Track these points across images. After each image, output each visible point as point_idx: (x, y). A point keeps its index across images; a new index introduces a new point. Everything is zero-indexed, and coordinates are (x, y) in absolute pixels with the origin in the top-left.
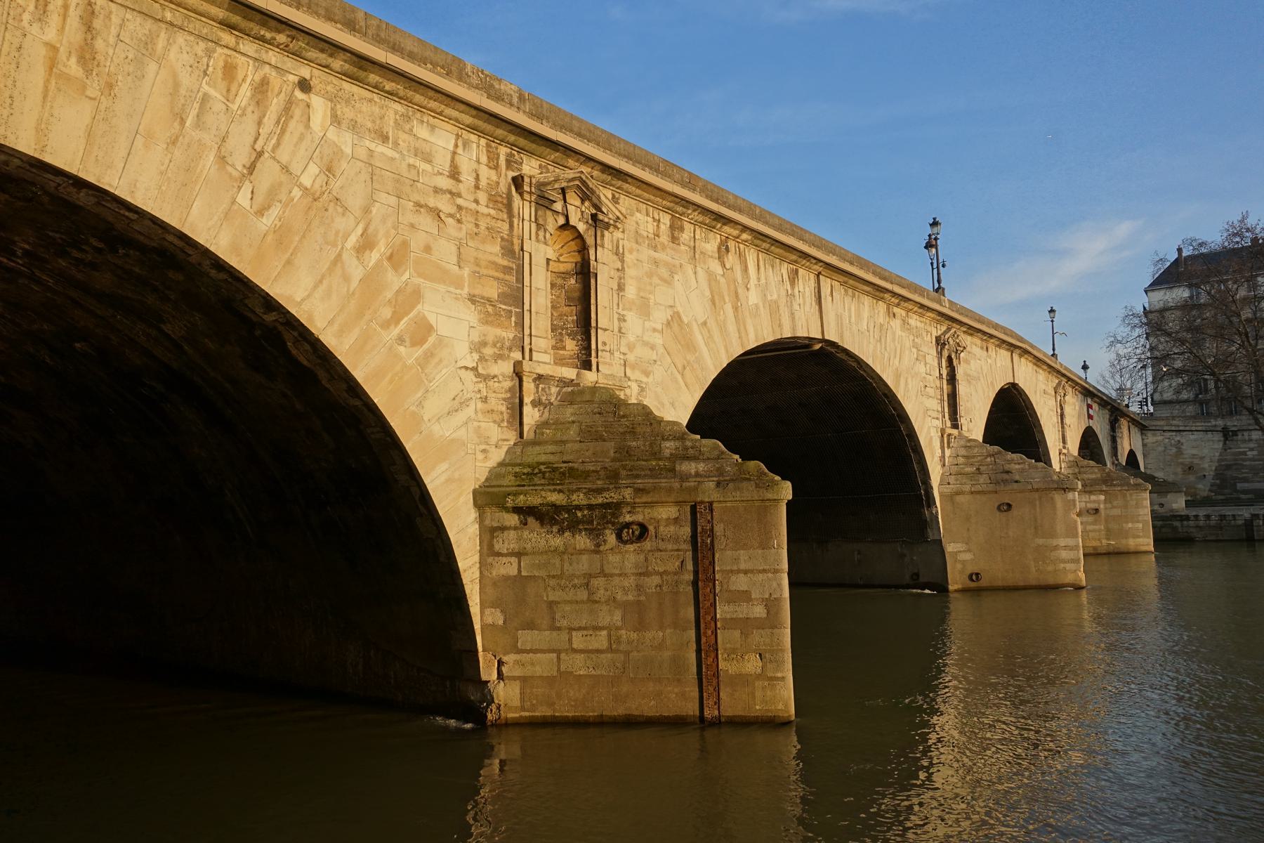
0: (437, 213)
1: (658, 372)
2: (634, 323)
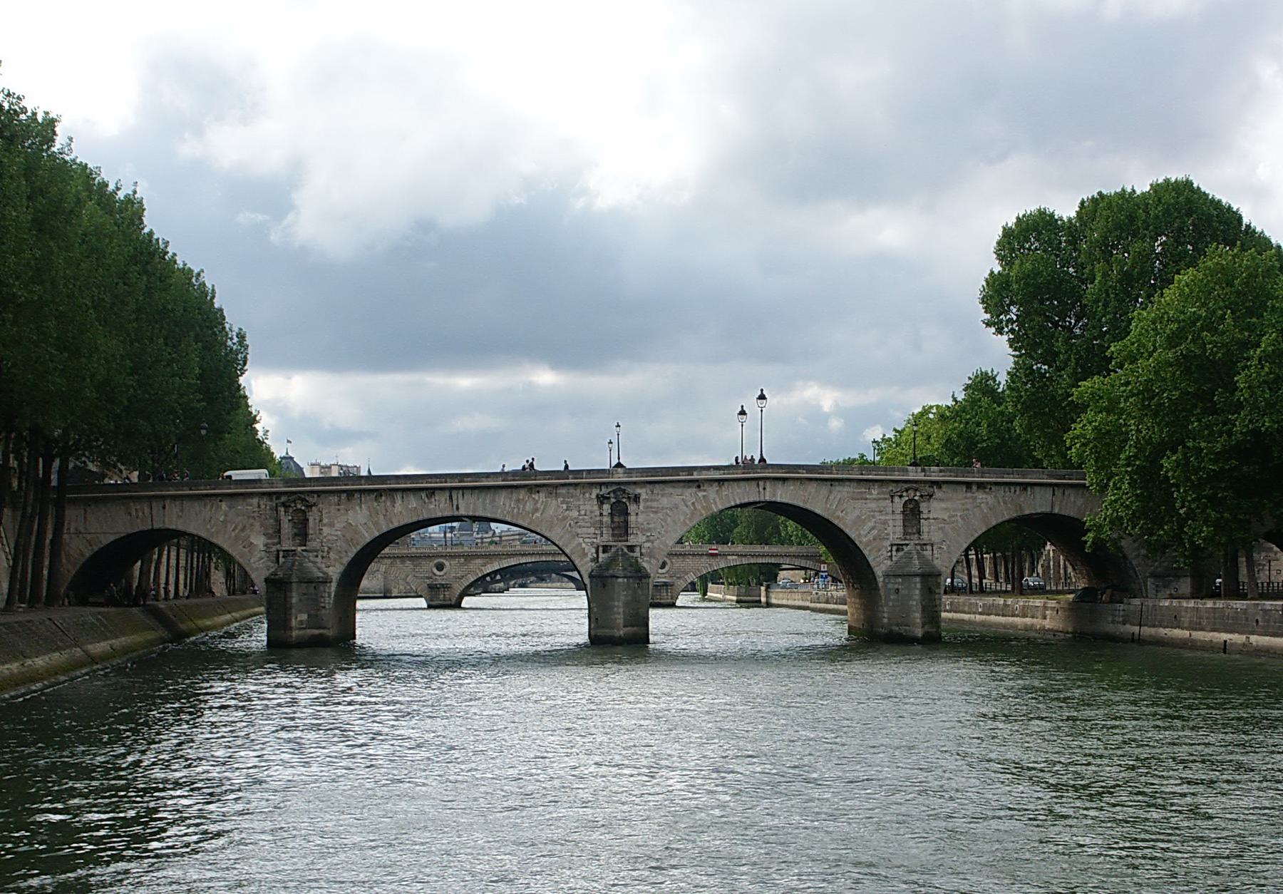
0: (253, 517)
2: (326, 530)
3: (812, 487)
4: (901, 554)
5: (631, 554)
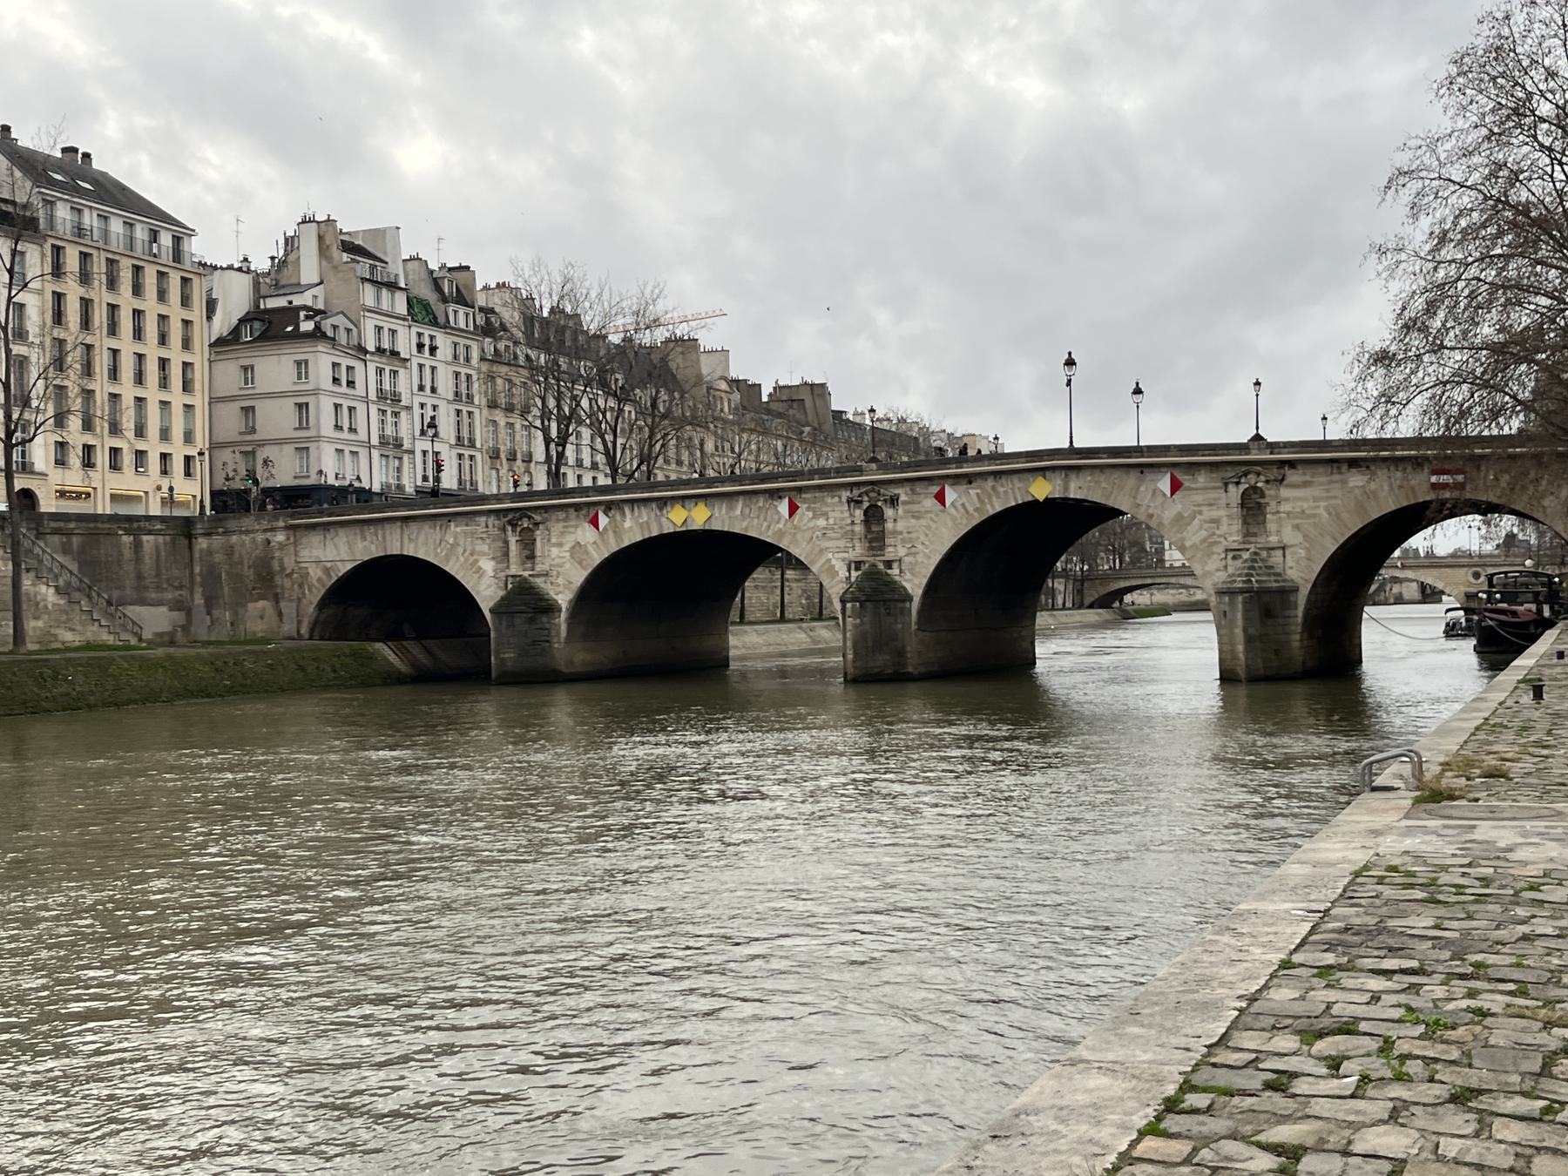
1: (568, 566)
4: (1239, 563)
5: (889, 571)
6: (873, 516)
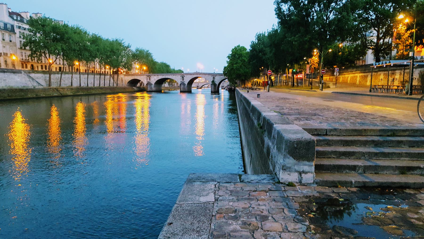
2: (152, 79)
3: (203, 75)
6: (183, 77)
